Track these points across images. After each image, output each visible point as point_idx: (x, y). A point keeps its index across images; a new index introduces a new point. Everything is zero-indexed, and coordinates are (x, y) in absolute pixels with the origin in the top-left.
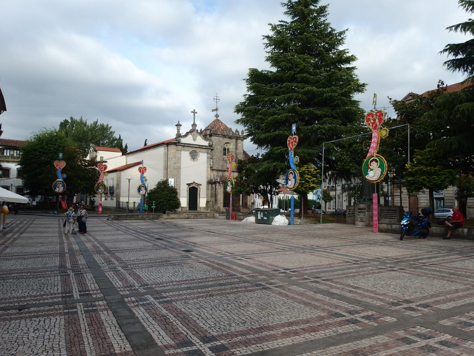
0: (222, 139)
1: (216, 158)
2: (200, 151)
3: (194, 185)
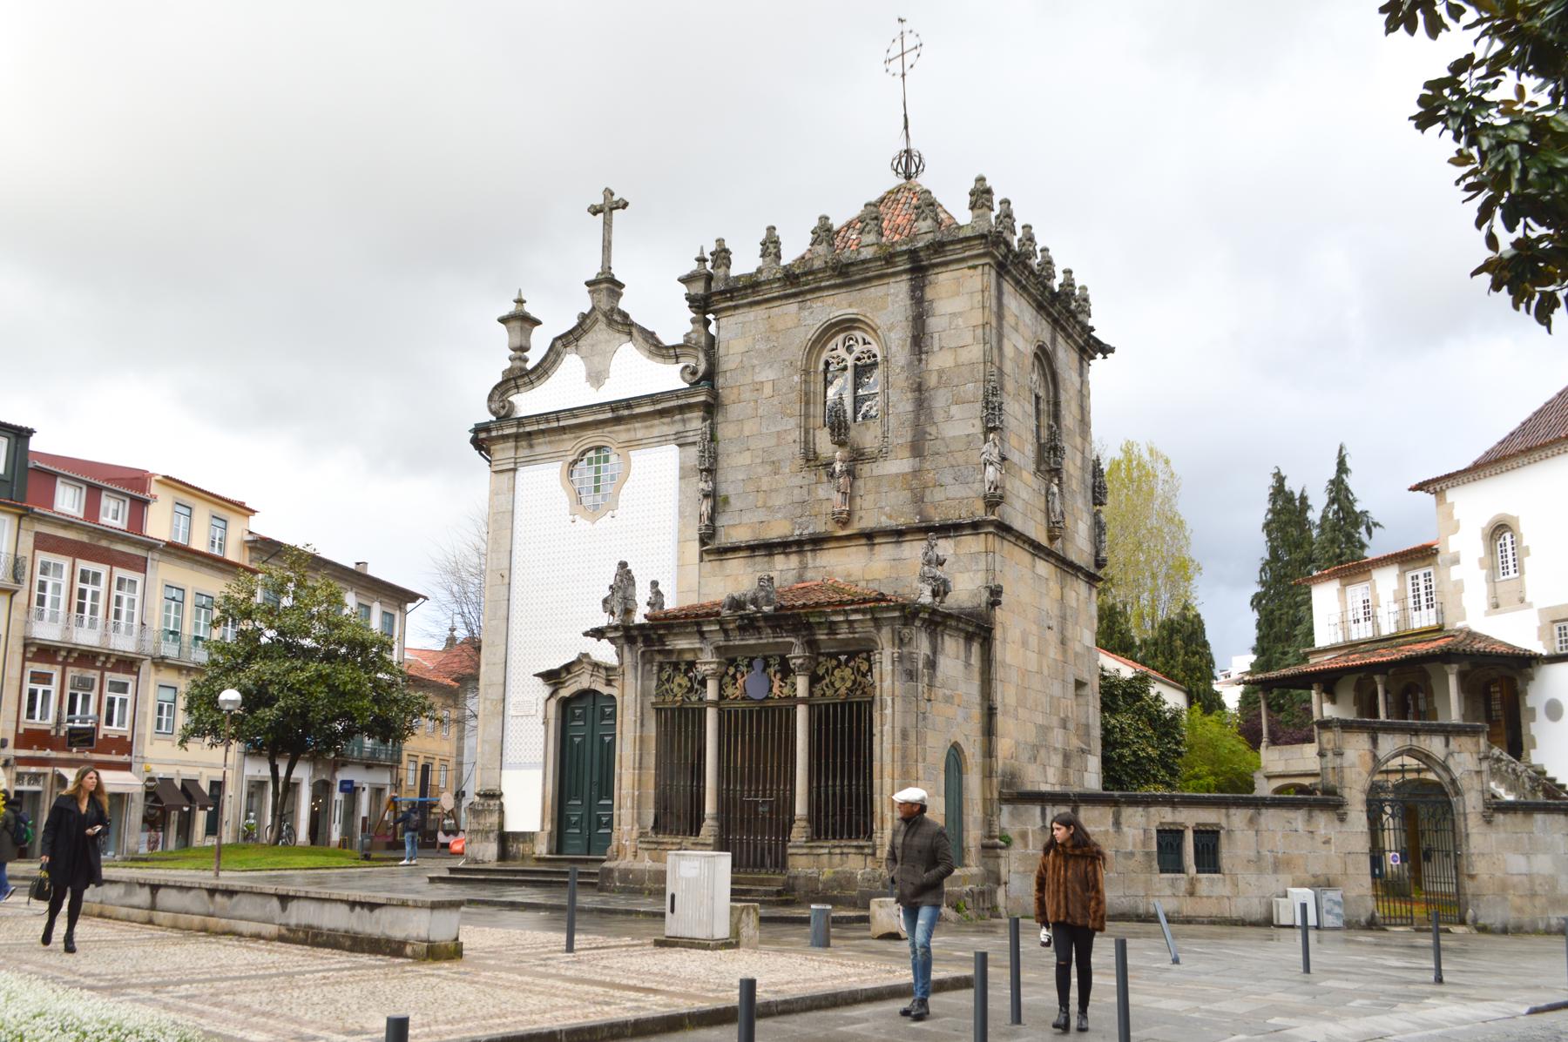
0: (792, 307)
1: (745, 459)
2: (632, 444)
3: (583, 681)
